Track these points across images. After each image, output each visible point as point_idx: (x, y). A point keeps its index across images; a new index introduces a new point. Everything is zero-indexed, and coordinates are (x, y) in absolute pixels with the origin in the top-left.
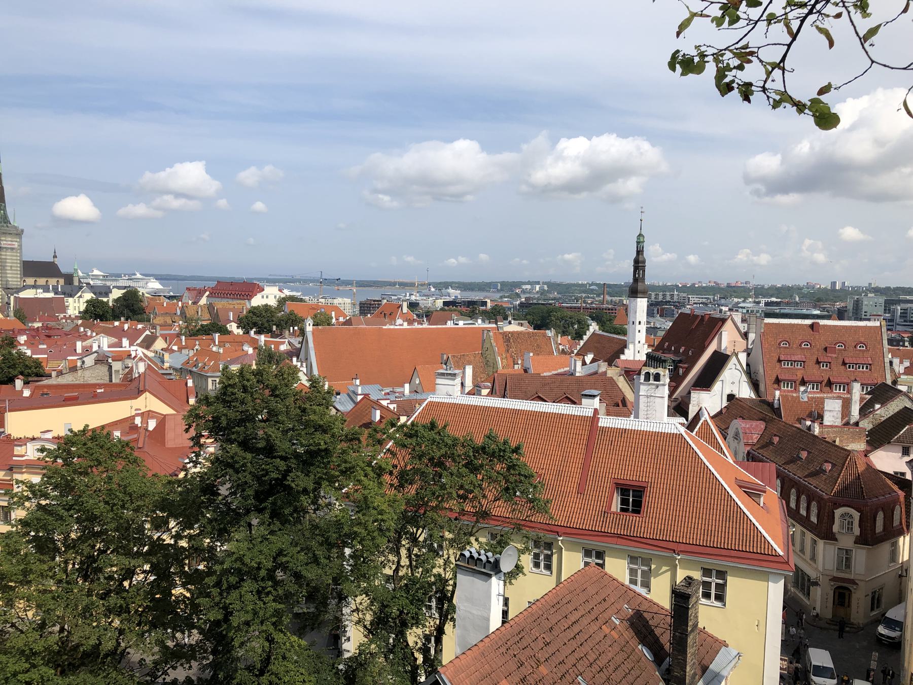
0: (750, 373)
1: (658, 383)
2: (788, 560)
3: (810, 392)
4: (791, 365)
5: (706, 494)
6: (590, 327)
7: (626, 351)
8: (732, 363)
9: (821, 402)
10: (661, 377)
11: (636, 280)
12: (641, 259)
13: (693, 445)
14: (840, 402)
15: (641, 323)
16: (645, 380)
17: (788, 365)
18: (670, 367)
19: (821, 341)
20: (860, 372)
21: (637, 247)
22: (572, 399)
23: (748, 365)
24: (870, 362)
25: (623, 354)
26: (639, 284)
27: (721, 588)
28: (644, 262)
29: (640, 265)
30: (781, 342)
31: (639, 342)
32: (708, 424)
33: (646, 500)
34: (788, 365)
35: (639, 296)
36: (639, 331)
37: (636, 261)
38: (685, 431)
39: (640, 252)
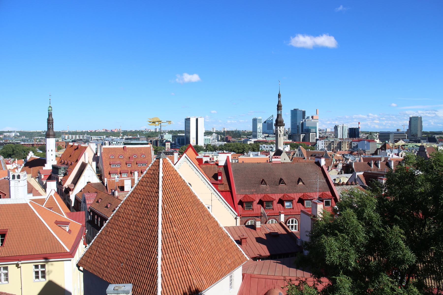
0: (99, 171)
1: (19, 179)
2: (72, 253)
3: (119, 178)
4: (115, 166)
5: (37, 230)
6: (29, 154)
7: (46, 165)
8: (88, 168)
9: (123, 182)
10: (21, 177)
11: (48, 129)
12: (51, 119)
13: (32, 208)
14: (130, 181)
15: (53, 151)
16: (12, 179)
17: (114, 166)
18: (63, 172)
19: (127, 155)
20: (143, 167)
21: (49, 113)
22: (3, 192)
23: (97, 167)
24: (147, 163)
25: (44, 166)
26: (51, 131)
27: (43, 272)
28: (53, 120)
29: (50, 121)
30: (110, 156)
31: (52, 160)
32: (52, 197)
33: (7, 237)
34: (114, 166)
35: (50, 137)
36: (52, 155)
37: (48, 120)
38: (30, 202)
39: (50, 115)
